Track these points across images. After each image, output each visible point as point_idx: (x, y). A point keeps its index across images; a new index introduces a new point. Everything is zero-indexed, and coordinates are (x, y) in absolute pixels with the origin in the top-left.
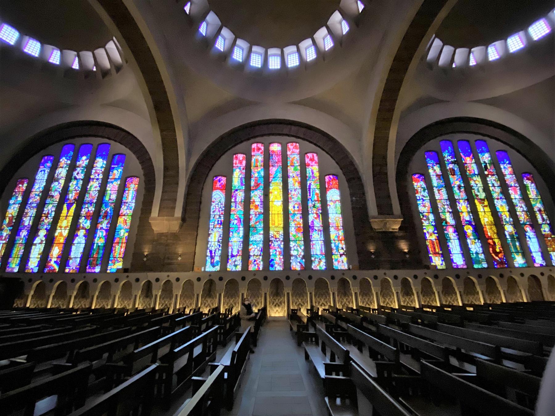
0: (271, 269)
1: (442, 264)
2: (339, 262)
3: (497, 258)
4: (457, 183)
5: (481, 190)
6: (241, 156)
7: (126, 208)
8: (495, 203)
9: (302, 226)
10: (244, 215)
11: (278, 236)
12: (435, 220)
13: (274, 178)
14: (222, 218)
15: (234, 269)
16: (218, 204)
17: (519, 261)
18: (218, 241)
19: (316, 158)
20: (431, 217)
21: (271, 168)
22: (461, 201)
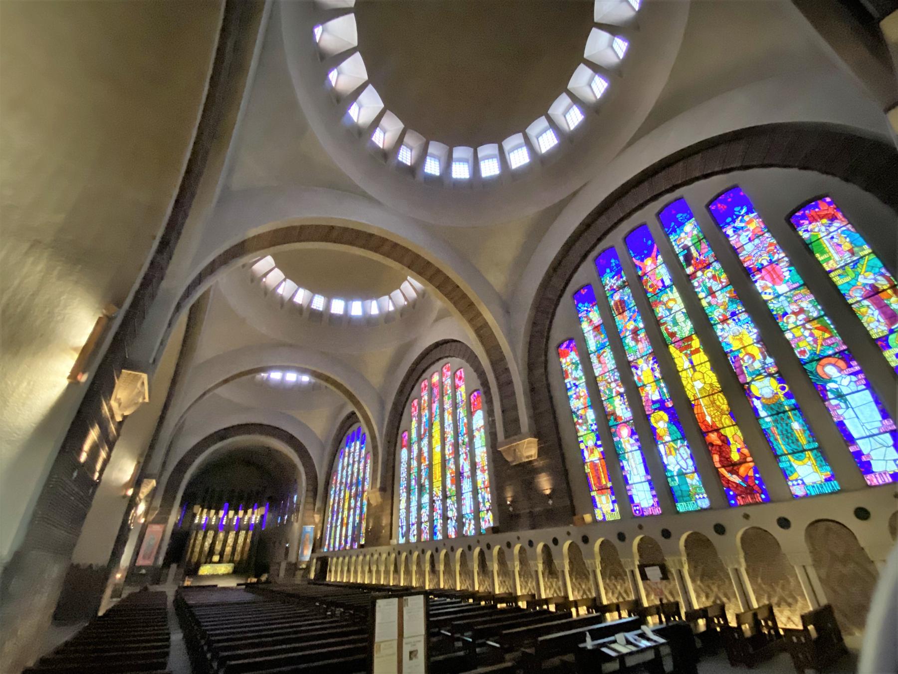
1: (613, 510)
2: (485, 521)
3: (735, 479)
4: (631, 325)
5: (680, 318)
8: (719, 333)
12: (596, 419)
17: (807, 474)
20: (591, 415)
22: (641, 362)
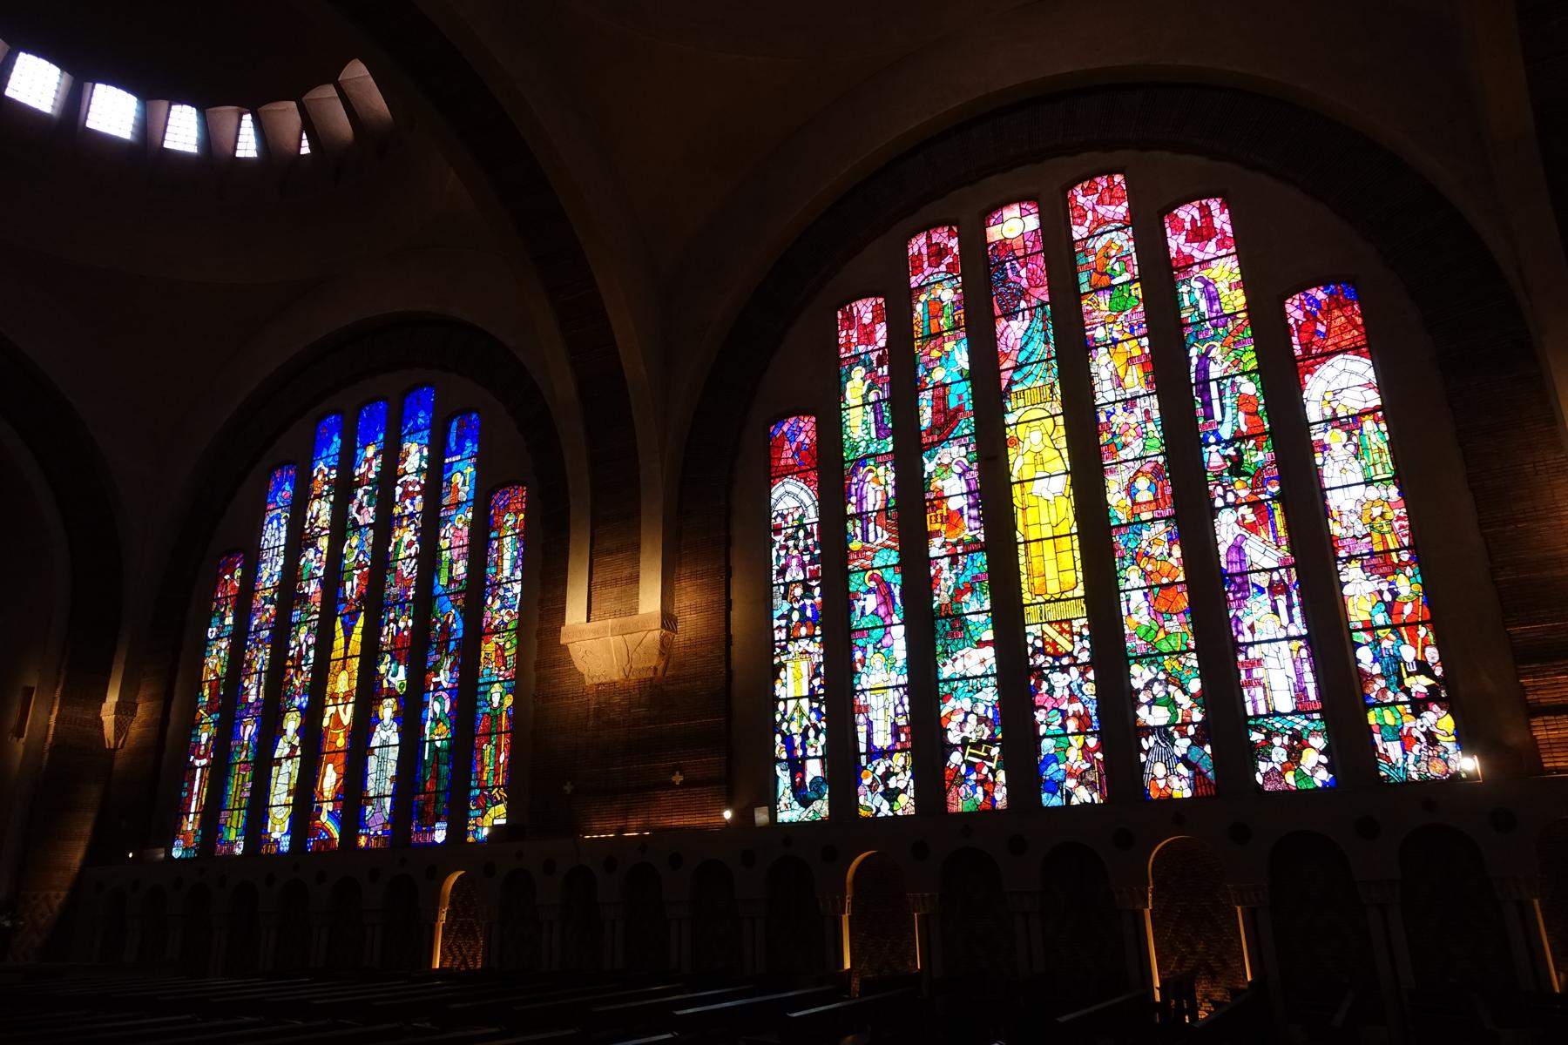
0: (1051, 801)
2: (1406, 741)
6: (865, 310)
7: (498, 604)
9: (1181, 578)
10: (903, 566)
11: (1064, 644)
13: (1017, 368)
14: (817, 591)
15: (885, 810)
16: (794, 537)
18: (812, 696)
19: (1221, 220)
21: (1001, 324)
